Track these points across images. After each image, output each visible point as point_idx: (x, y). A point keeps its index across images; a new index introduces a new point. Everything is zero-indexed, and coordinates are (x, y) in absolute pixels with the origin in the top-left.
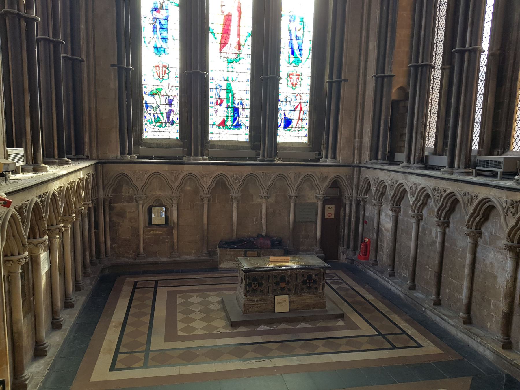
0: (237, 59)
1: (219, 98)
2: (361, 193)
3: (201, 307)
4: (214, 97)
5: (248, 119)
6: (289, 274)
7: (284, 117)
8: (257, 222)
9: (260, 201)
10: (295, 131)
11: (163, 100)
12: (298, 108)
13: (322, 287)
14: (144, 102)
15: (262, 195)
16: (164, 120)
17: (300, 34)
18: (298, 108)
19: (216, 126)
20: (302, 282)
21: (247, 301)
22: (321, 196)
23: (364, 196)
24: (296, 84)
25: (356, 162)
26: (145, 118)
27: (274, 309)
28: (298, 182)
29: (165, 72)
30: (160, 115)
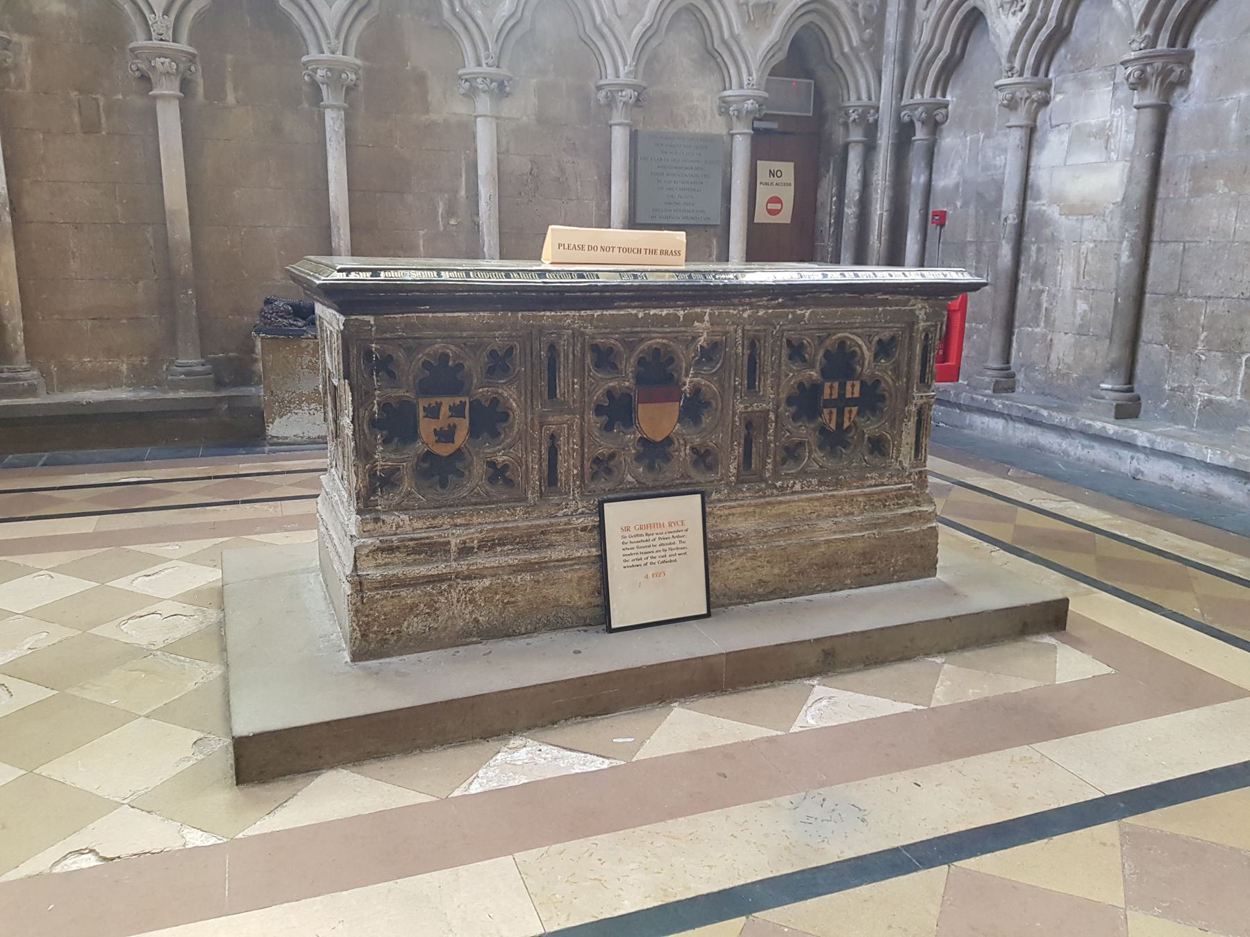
2: (919, 84)
3: (44, 637)
6: (702, 341)
8: (453, 222)
9: (460, 108)
13: (913, 433)
15: (471, 68)
20: (790, 401)
21: (381, 558)
22: (748, 98)
23: (934, 95)
27: (598, 600)
28: (642, 15)
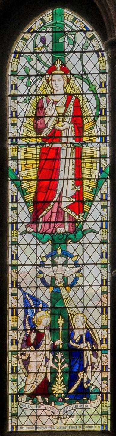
1: (34, 328)
4: (22, 328)
5: (108, 375)
19: (25, 396)
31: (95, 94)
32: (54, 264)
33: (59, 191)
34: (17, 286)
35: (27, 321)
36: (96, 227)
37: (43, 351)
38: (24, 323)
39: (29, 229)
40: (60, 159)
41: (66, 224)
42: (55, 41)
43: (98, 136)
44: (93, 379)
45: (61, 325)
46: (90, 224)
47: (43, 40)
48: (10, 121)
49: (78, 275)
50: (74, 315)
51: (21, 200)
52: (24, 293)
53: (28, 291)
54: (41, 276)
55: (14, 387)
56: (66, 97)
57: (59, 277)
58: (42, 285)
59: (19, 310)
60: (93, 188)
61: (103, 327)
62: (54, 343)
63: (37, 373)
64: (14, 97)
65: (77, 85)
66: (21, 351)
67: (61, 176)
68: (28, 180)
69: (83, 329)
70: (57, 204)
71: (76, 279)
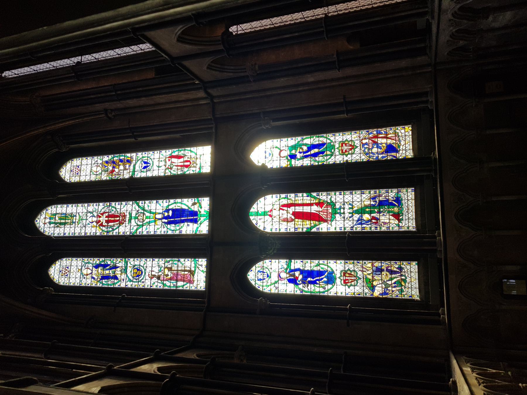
0: (332, 204)
1: (370, 221)
4: (370, 225)
7: (385, 153)
10: (399, 140)
11: (376, 277)
12: (376, 140)
14: (381, 296)
16: (398, 277)
17: (305, 148)
18: (376, 140)
19: (400, 223)
24: (351, 145)
25: (429, 69)
26: (397, 296)
29: (349, 274)
30: (393, 281)
31: (280, 200)
32: (344, 213)
33: (315, 212)
34: (353, 228)
35: (367, 223)
36: (329, 197)
37: (380, 217)
38: (368, 225)
39: (330, 223)
40: (303, 212)
41: (328, 209)
42: (261, 215)
43: (295, 198)
44: (391, 196)
45: (369, 210)
46: (328, 199)
47: (260, 219)
48: (288, 231)
49: (348, 203)
50: (365, 205)
51: (318, 227)
52: (355, 225)
53: (355, 223)
54: (348, 218)
55: (396, 228)
56: (280, 210)
57: (349, 211)
58: (352, 218)
59: (363, 226)
60: (314, 199)
61: (370, 193)
62: (376, 212)
63: (389, 219)
64: (280, 230)
65: (277, 207)
66: (380, 226)
67: (310, 211)
68: (311, 224)
69: (370, 201)
70: (320, 213)
71: (350, 204)
